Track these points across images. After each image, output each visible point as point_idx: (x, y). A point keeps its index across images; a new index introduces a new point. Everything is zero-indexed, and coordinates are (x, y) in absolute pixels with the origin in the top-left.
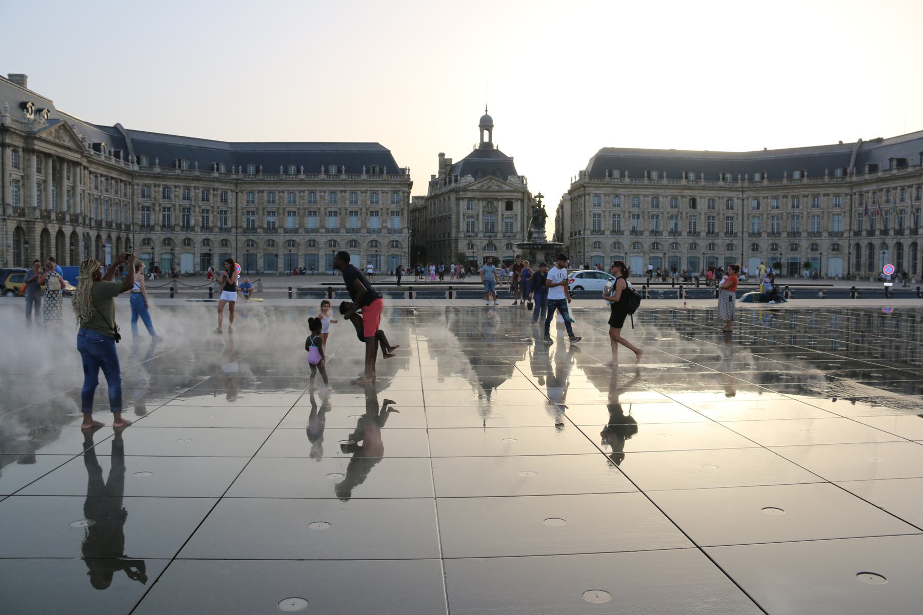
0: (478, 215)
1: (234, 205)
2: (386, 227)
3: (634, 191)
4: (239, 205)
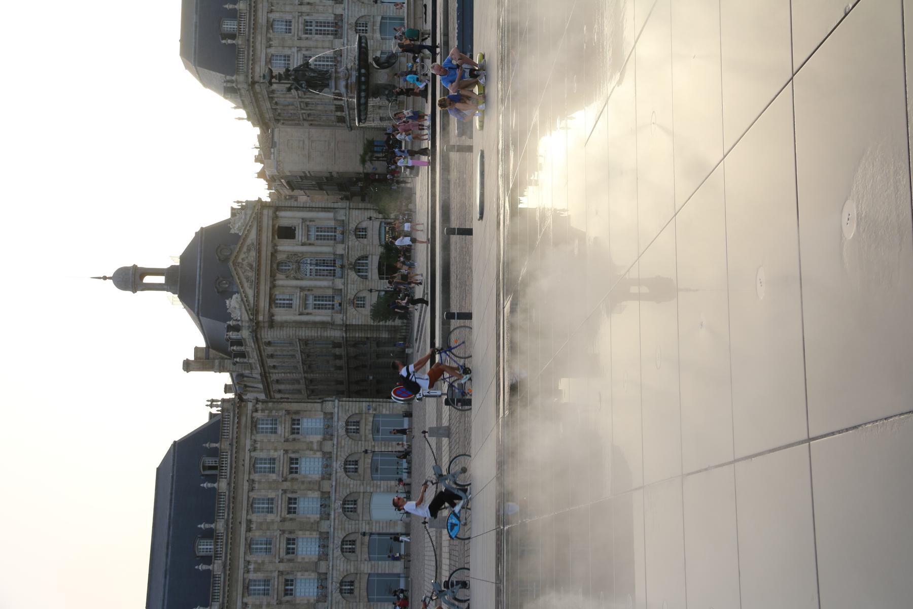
0: (302, 289)
2: (321, 444)
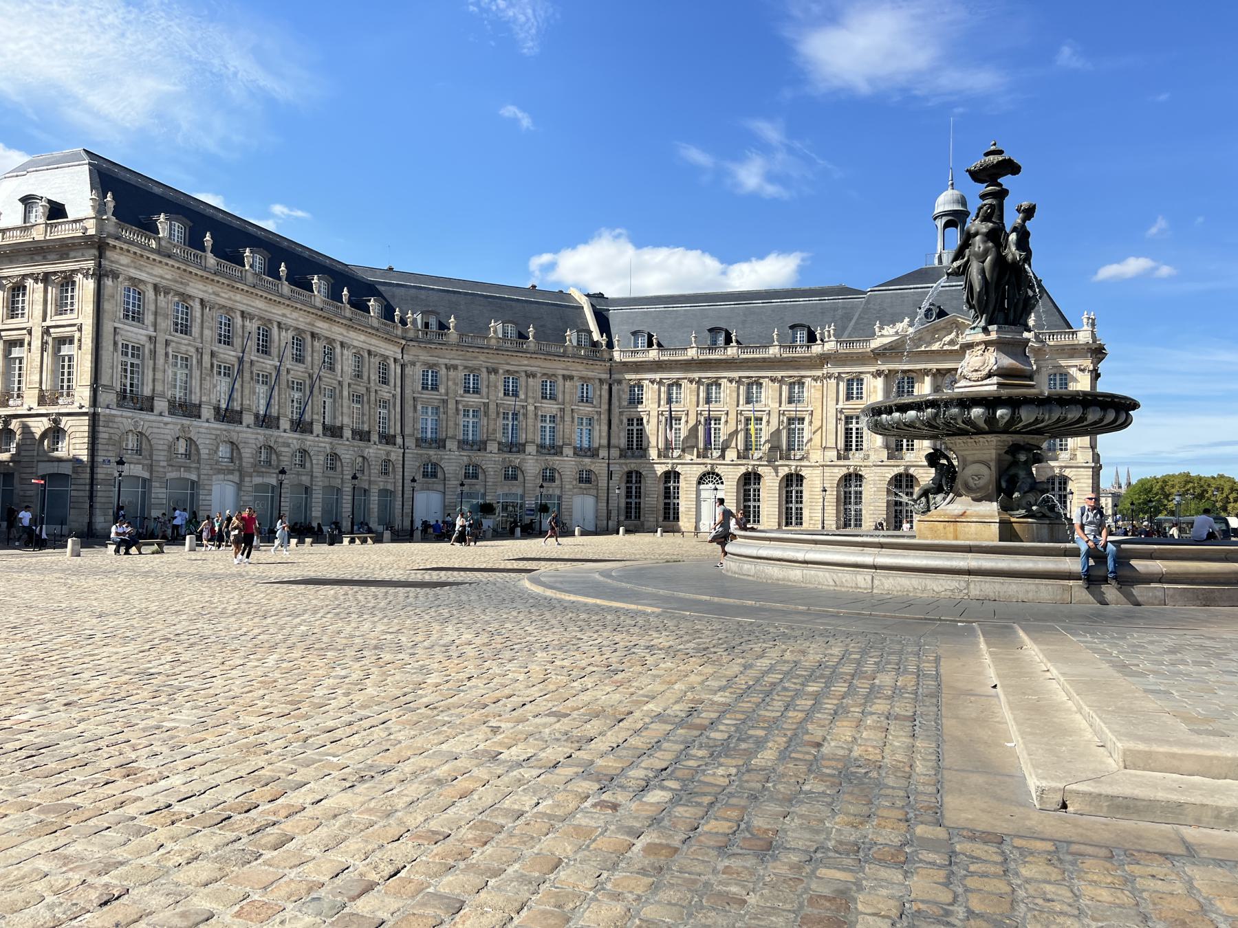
3: (225, 297)
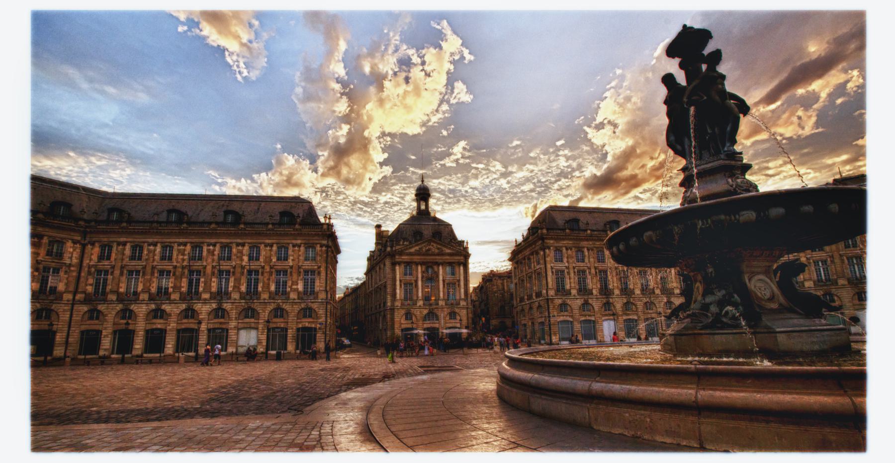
0: (416, 281)
1: (75, 261)
4: (86, 262)
